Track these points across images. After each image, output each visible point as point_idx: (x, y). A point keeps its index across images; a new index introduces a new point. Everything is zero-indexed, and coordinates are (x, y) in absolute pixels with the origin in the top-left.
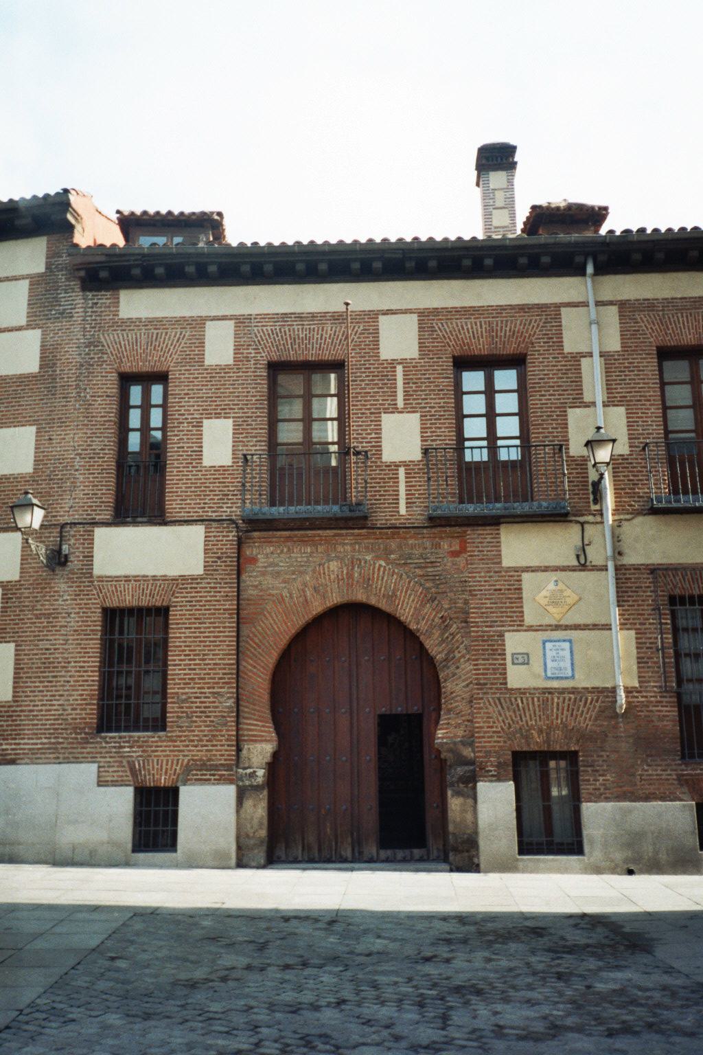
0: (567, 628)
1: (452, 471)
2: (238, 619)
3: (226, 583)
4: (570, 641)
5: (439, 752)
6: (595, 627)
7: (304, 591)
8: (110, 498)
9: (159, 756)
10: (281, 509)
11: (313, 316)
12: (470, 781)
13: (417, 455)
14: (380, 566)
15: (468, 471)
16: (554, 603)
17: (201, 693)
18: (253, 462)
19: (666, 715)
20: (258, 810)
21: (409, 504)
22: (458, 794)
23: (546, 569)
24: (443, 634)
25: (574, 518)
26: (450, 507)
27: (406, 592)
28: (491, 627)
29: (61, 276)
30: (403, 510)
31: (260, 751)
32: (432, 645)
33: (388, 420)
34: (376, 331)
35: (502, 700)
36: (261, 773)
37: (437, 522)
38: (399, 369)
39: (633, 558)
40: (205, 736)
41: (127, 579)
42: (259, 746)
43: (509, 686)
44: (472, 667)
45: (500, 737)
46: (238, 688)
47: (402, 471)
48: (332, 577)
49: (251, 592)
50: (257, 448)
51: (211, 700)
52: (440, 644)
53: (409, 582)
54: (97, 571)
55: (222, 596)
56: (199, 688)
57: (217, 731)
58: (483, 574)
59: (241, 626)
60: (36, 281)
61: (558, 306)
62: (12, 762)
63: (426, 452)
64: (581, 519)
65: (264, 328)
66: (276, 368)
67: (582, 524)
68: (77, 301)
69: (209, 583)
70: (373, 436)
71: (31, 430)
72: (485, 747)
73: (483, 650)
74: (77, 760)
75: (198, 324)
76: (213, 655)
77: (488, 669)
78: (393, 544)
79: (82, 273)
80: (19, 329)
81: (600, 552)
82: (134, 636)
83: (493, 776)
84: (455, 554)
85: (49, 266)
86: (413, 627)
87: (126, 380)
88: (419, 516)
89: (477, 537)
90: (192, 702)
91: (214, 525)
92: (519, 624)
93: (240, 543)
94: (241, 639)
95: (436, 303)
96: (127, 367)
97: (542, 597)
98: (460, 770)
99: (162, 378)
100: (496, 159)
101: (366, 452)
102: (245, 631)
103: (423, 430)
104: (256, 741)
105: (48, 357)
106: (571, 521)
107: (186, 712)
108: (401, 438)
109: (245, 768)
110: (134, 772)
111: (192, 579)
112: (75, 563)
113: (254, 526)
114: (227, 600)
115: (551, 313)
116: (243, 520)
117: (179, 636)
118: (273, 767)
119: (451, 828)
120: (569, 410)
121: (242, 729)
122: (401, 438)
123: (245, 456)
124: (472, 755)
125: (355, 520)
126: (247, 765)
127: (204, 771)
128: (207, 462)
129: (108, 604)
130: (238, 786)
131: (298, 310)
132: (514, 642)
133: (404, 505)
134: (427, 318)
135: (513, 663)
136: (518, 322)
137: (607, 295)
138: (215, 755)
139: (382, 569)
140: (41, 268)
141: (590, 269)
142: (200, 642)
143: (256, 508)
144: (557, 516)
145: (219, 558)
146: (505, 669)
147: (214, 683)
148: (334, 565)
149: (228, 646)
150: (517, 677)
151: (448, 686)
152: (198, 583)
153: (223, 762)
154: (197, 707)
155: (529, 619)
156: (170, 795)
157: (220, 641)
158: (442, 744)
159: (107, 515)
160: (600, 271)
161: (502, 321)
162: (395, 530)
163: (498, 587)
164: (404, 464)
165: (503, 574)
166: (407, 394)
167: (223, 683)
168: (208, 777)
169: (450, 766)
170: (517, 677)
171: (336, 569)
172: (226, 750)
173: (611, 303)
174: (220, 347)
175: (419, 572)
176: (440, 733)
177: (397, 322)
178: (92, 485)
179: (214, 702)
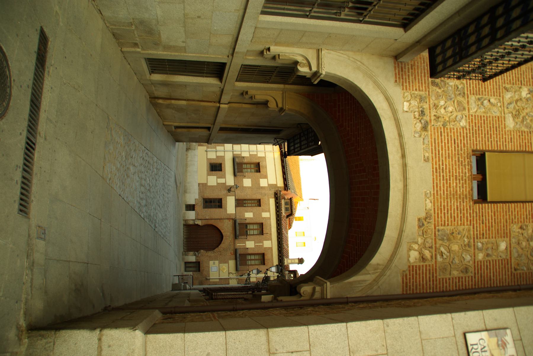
9: (199, 208)
11: (271, 230)
12: (195, 255)
20: (191, 223)
26: (239, 252)
29: (277, 189)
31: (199, 223)
37: (236, 250)
50: (247, 221)
60: (276, 185)
66: (262, 224)
68: (272, 192)
71: (251, 186)
75: (269, 211)
81: (231, 276)
82: (218, 203)
89: (233, 256)
92: (220, 263)
95: (274, 250)
97: (224, 267)
98: (197, 253)
112: (229, 194)
113: (235, 221)
117: (218, 210)
118: (197, 225)
122: (250, 244)
125: (236, 237)
127: (197, 214)
128: (246, 213)
133: (239, 245)
134: (271, 249)
144: (237, 270)
150: (211, 263)
151: (210, 252)
155: (220, 265)
156: (194, 210)
159: (237, 198)
162: (234, 243)
170: (211, 263)
174: (265, 215)
177: (270, 244)
178: (241, 195)
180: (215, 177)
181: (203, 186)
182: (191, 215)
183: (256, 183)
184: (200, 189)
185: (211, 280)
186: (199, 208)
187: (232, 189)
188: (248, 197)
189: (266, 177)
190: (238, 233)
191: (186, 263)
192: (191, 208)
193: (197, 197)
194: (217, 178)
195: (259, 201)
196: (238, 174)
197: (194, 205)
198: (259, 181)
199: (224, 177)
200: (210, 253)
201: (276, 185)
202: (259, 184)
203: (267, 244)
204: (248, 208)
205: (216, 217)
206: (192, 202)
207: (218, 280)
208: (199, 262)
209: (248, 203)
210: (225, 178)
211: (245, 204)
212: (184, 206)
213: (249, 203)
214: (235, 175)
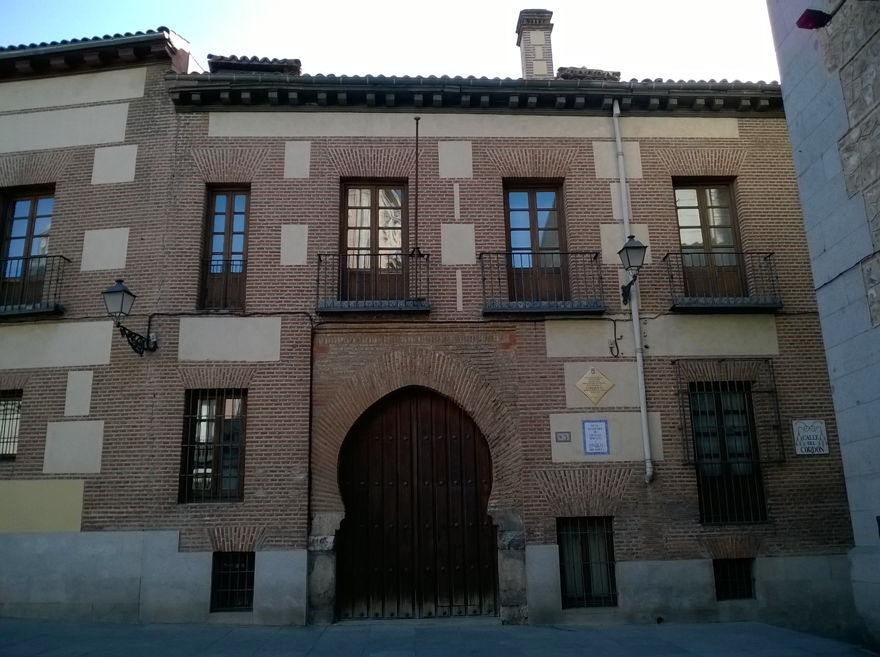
0: (602, 410)
1: (504, 274)
2: (311, 401)
3: (300, 369)
4: (606, 422)
5: (490, 518)
6: (626, 409)
7: (371, 377)
8: (194, 291)
9: (234, 526)
10: (352, 303)
11: (381, 140)
12: (519, 546)
13: (471, 259)
14: (440, 355)
15: (514, 275)
16: (593, 389)
17: (276, 467)
18: (326, 262)
19: (685, 485)
20: (326, 571)
21: (466, 302)
22: (510, 556)
23: (584, 360)
24: (494, 416)
25: (607, 317)
27: (463, 378)
28: (538, 409)
30: (460, 307)
31: (329, 521)
32: (484, 424)
33: (446, 230)
34: (436, 154)
35: (548, 474)
36: (331, 539)
37: (491, 315)
38: (456, 187)
39: (656, 351)
40: (280, 506)
41: (209, 364)
42: (329, 515)
43: (553, 461)
44: (520, 444)
45: (545, 505)
46: (310, 462)
47: (459, 273)
48: (397, 364)
49: (322, 377)
51: (286, 473)
52: (492, 424)
53: (466, 370)
54: (182, 356)
55: (297, 381)
56: (274, 463)
57: (291, 501)
58: (530, 363)
59: (314, 407)
60: (134, 104)
61: (590, 140)
62: (100, 529)
63: (480, 256)
64: (614, 317)
65: (337, 149)
67: (615, 321)
68: (170, 119)
69: (285, 369)
70: (434, 242)
72: (533, 514)
73: (531, 429)
74: (159, 528)
75: (279, 143)
76: (288, 433)
77: (536, 446)
78: (451, 336)
79: (177, 96)
80: (118, 144)
83: (540, 539)
84: (506, 346)
85: (147, 93)
86: (469, 409)
87: (213, 189)
88: (476, 312)
89: (524, 329)
90: (268, 476)
91: (291, 317)
92: (562, 407)
93: (313, 334)
94: (313, 419)
96: (214, 179)
97: (582, 382)
98: (509, 536)
99: (245, 188)
100: (534, 22)
101: (428, 255)
102: (317, 412)
103: (477, 238)
104: (326, 510)
105: (143, 169)
106: (605, 319)
107: (263, 485)
108: (457, 246)
109: (315, 536)
110: (213, 540)
111: (269, 365)
114: (301, 384)
115: (585, 146)
116: (317, 313)
119: (502, 586)
120: (601, 226)
121: (314, 500)
122: (457, 246)
123: (319, 255)
124: (521, 521)
125: (420, 313)
126: (318, 532)
127: (277, 539)
128: (284, 262)
129: (191, 387)
130: (309, 552)
131: (368, 135)
132: (558, 423)
133: (461, 301)
134: (480, 145)
135: (557, 441)
136: (557, 152)
137: (629, 134)
138: (289, 523)
139: (441, 358)
140: (141, 94)
141: (617, 110)
142: (276, 421)
143: (329, 303)
145: (293, 346)
146: (550, 446)
147: (289, 458)
148: (398, 355)
149: (301, 425)
150: (560, 453)
151: (498, 461)
152: (274, 369)
153: (296, 529)
154: (272, 480)
155: (570, 403)
156: (248, 558)
157: (294, 421)
158: (494, 512)
159: (192, 307)
160: (626, 111)
161: (543, 151)
162: (454, 324)
163: (543, 375)
164: (461, 267)
165: (548, 363)
166: (463, 209)
167: (297, 458)
168: (282, 543)
169: (502, 531)
170: (560, 453)
171: (400, 358)
172: (299, 519)
173: (633, 140)
174: (297, 164)
175: (474, 361)
176: (492, 503)
177: (455, 146)
179: (288, 475)
180: (52, 427)
181: (105, 501)
182: (282, 573)
183: (113, 206)
184: (120, 523)
185: (660, 457)
186: (234, 526)
187: (138, 327)
188: (192, 244)
189: (84, 157)
190: (401, 304)
191: (569, 601)
192: (232, 579)
193: (168, 539)
194: (59, 415)
195: (213, 189)
196: (48, 299)
197: (220, 558)
198: (102, 187)
199: (55, 381)
200: (507, 458)
201: (134, 104)
202: (120, 189)
203: (455, 163)
204: (253, 249)
205: (302, 425)
206: (199, 569)
207: (657, 416)
208: (562, 522)
209: (228, 251)
210: (64, 372)
211: (228, 263)
212: (225, 618)
213: (228, 244)
214: (57, 314)
